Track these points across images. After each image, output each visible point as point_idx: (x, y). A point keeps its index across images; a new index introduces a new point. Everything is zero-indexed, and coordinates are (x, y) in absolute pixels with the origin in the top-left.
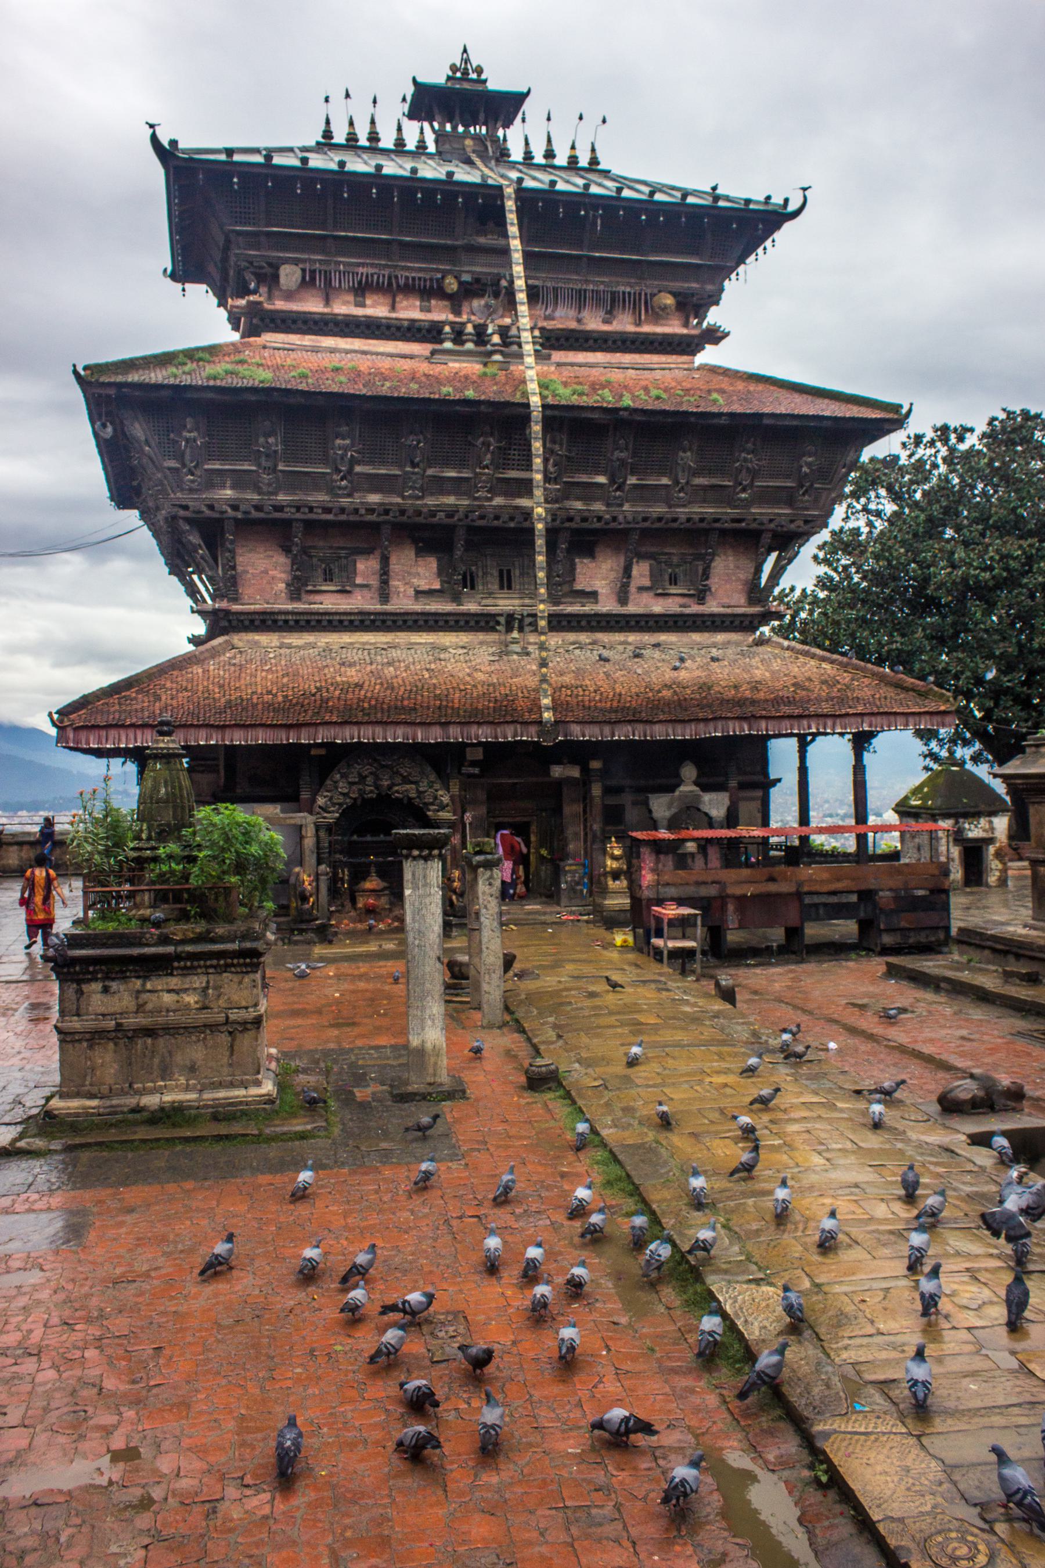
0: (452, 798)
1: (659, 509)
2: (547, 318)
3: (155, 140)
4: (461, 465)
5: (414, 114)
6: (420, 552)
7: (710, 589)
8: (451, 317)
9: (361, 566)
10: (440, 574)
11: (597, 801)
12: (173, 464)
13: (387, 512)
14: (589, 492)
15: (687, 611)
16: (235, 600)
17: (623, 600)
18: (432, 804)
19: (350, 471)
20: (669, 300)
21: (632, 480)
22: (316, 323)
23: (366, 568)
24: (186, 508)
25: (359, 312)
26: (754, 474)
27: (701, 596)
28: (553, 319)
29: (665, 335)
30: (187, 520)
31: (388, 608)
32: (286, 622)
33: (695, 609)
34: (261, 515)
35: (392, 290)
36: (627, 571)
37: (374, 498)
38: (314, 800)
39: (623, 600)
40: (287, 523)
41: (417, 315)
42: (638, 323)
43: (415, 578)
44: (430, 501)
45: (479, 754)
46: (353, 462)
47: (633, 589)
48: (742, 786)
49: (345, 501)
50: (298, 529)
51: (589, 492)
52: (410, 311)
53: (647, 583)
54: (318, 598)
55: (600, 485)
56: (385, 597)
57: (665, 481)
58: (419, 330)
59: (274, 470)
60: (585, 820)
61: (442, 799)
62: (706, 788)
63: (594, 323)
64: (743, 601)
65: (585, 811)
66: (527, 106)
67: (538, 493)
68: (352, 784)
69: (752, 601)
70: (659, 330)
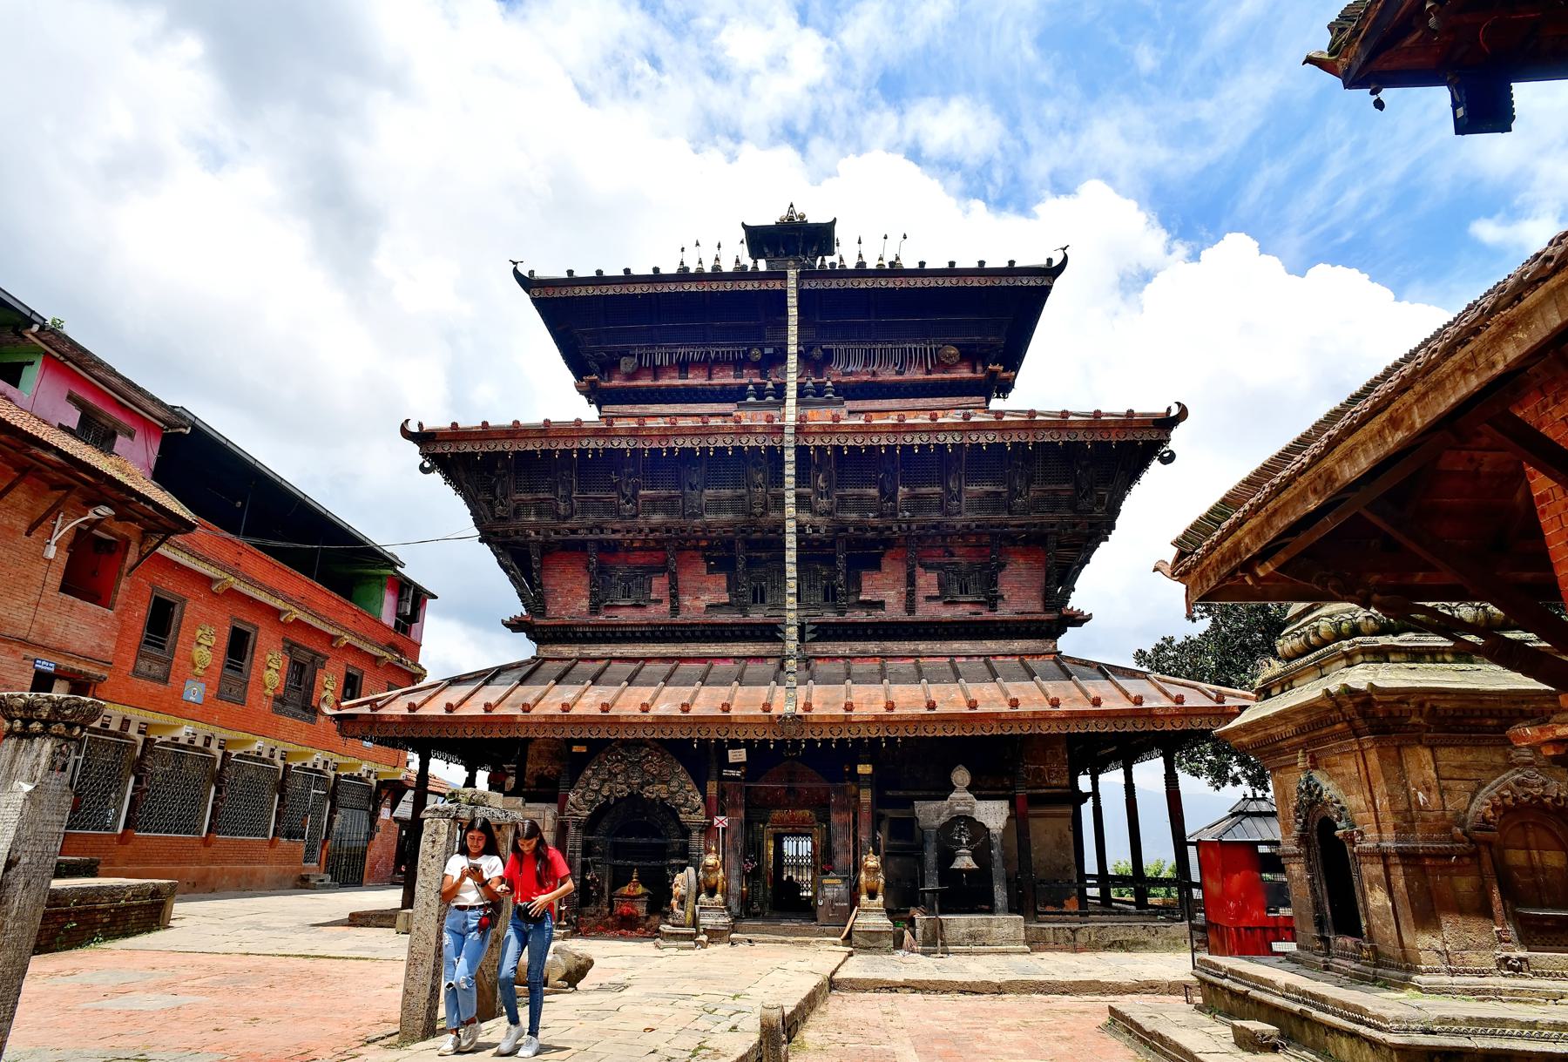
0: (704, 800)
1: (936, 516)
2: (845, 374)
3: (516, 273)
4: (737, 485)
5: (755, 253)
6: (710, 570)
7: (1001, 597)
8: (758, 380)
9: (656, 583)
10: (729, 590)
11: (866, 809)
12: (488, 497)
13: (668, 531)
14: (861, 503)
15: (978, 617)
16: (542, 615)
17: (910, 608)
18: (683, 805)
19: (635, 495)
20: (953, 351)
21: (902, 491)
22: (644, 393)
23: (659, 584)
24: (496, 534)
25: (680, 382)
26: (1030, 481)
27: (992, 602)
28: (851, 374)
29: (953, 381)
30: (498, 544)
31: (678, 620)
32: (584, 633)
33: (986, 615)
34: (559, 537)
35: (709, 365)
36: (911, 581)
37: (657, 518)
38: (566, 797)
39: (910, 608)
40: (582, 546)
41: (731, 381)
42: (929, 372)
43: (704, 597)
44: (709, 517)
45: (738, 756)
46: (637, 487)
47: (920, 596)
48: (1035, 801)
49: (629, 523)
50: (591, 548)
51: (861, 503)
52: (725, 379)
53: (936, 593)
54: (615, 612)
55: (874, 498)
56: (675, 610)
57: (938, 489)
58: (731, 392)
59: (568, 498)
60: (856, 831)
61: (690, 801)
62: (979, 798)
63: (888, 375)
64: (1038, 607)
65: (855, 822)
66: (839, 232)
67: (790, 498)
68: (605, 781)
69: (1047, 609)
70: (946, 376)
